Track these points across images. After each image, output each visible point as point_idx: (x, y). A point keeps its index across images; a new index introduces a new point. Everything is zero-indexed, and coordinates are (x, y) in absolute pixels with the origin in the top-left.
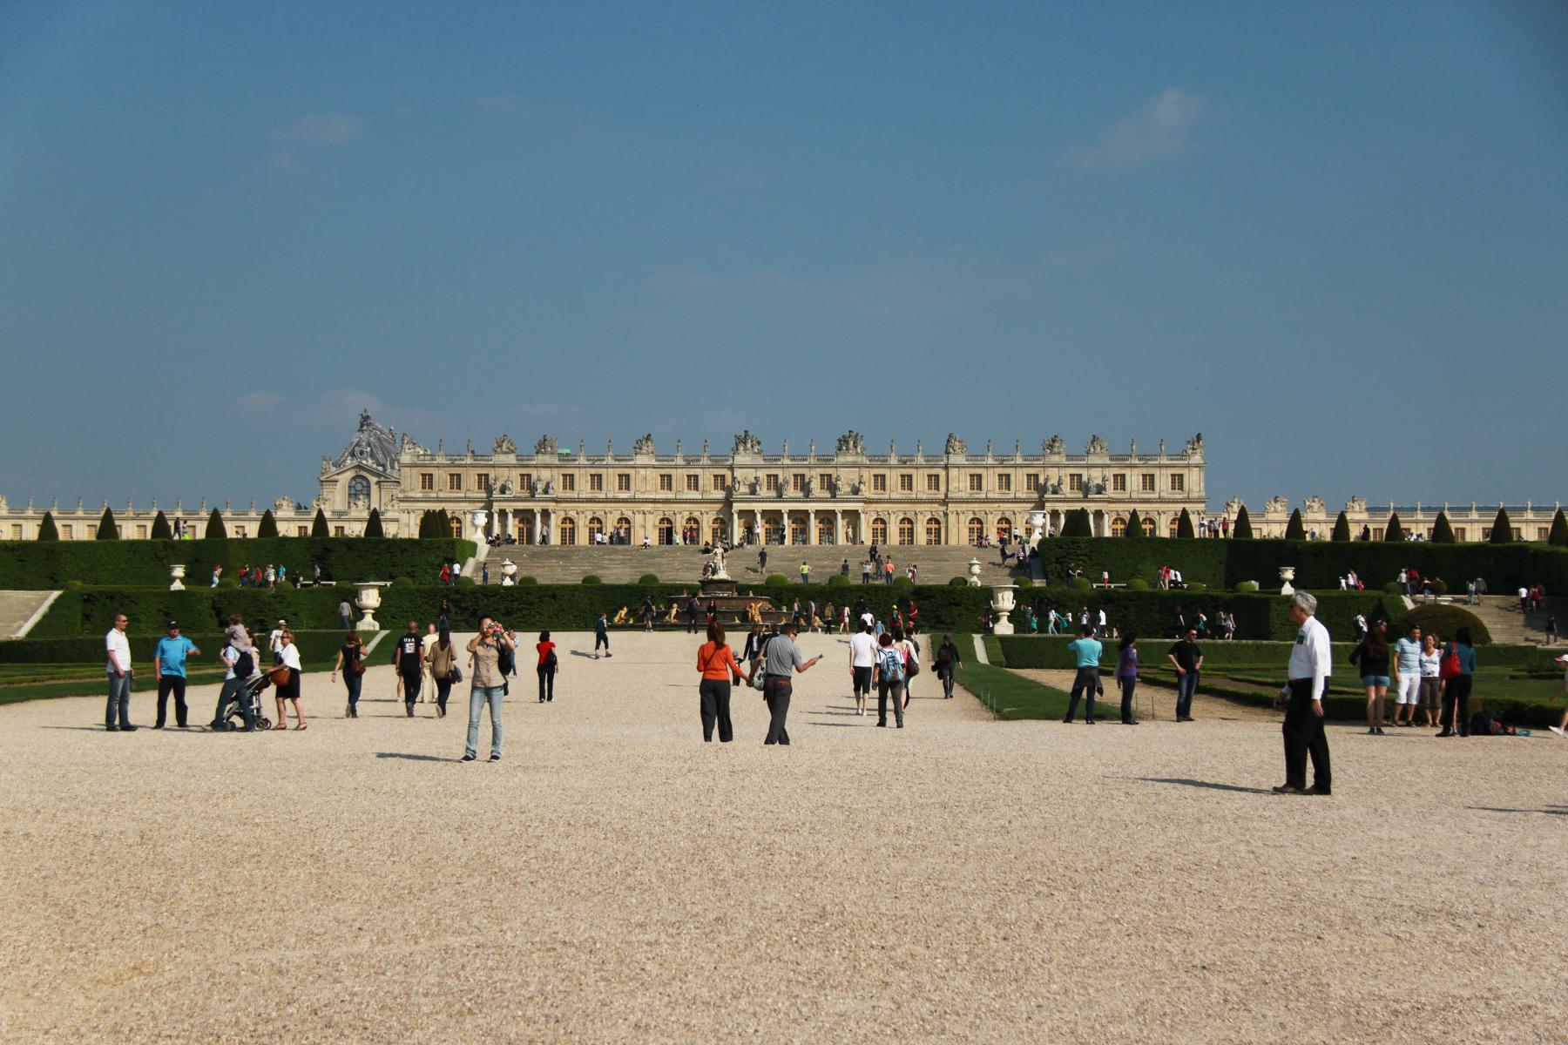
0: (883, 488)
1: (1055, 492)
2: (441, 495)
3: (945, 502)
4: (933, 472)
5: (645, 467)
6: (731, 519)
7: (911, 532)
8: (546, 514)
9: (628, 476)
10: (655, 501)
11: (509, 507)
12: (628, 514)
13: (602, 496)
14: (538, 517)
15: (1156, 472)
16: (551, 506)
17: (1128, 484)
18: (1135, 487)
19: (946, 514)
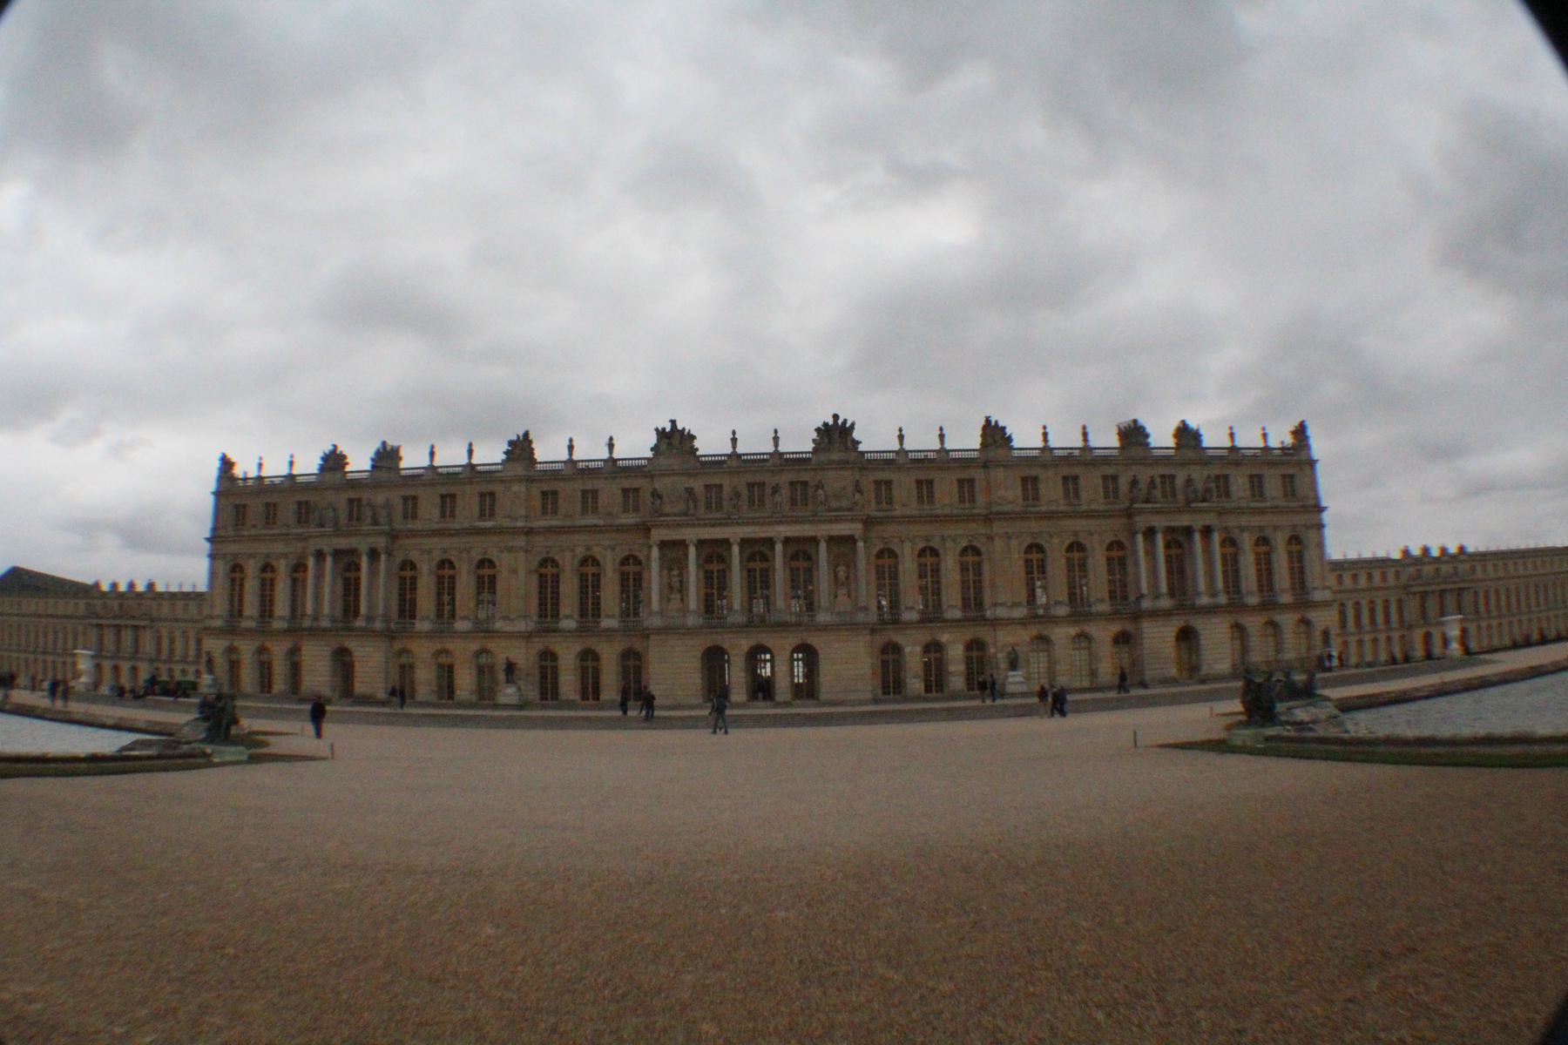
0: (890, 502)
1: (1147, 501)
2: (253, 532)
3: (988, 519)
4: (965, 475)
5: (519, 479)
6: (648, 558)
7: (936, 571)
8: (374, 554)
9: (492, 494)
10: (529, 532)
11: (327, 545)
12: (493, 554)
13: (455, 525)
14: (364, 562)
15: (1265, 471)
16: (381, 542)
17: (1233, 488)
18: (1241, 494)
19: (991, 538)
